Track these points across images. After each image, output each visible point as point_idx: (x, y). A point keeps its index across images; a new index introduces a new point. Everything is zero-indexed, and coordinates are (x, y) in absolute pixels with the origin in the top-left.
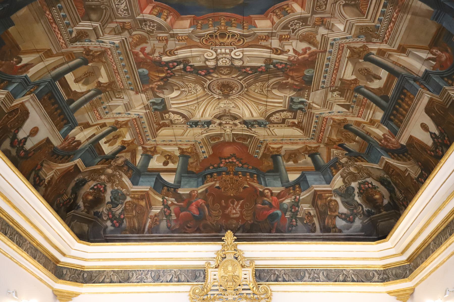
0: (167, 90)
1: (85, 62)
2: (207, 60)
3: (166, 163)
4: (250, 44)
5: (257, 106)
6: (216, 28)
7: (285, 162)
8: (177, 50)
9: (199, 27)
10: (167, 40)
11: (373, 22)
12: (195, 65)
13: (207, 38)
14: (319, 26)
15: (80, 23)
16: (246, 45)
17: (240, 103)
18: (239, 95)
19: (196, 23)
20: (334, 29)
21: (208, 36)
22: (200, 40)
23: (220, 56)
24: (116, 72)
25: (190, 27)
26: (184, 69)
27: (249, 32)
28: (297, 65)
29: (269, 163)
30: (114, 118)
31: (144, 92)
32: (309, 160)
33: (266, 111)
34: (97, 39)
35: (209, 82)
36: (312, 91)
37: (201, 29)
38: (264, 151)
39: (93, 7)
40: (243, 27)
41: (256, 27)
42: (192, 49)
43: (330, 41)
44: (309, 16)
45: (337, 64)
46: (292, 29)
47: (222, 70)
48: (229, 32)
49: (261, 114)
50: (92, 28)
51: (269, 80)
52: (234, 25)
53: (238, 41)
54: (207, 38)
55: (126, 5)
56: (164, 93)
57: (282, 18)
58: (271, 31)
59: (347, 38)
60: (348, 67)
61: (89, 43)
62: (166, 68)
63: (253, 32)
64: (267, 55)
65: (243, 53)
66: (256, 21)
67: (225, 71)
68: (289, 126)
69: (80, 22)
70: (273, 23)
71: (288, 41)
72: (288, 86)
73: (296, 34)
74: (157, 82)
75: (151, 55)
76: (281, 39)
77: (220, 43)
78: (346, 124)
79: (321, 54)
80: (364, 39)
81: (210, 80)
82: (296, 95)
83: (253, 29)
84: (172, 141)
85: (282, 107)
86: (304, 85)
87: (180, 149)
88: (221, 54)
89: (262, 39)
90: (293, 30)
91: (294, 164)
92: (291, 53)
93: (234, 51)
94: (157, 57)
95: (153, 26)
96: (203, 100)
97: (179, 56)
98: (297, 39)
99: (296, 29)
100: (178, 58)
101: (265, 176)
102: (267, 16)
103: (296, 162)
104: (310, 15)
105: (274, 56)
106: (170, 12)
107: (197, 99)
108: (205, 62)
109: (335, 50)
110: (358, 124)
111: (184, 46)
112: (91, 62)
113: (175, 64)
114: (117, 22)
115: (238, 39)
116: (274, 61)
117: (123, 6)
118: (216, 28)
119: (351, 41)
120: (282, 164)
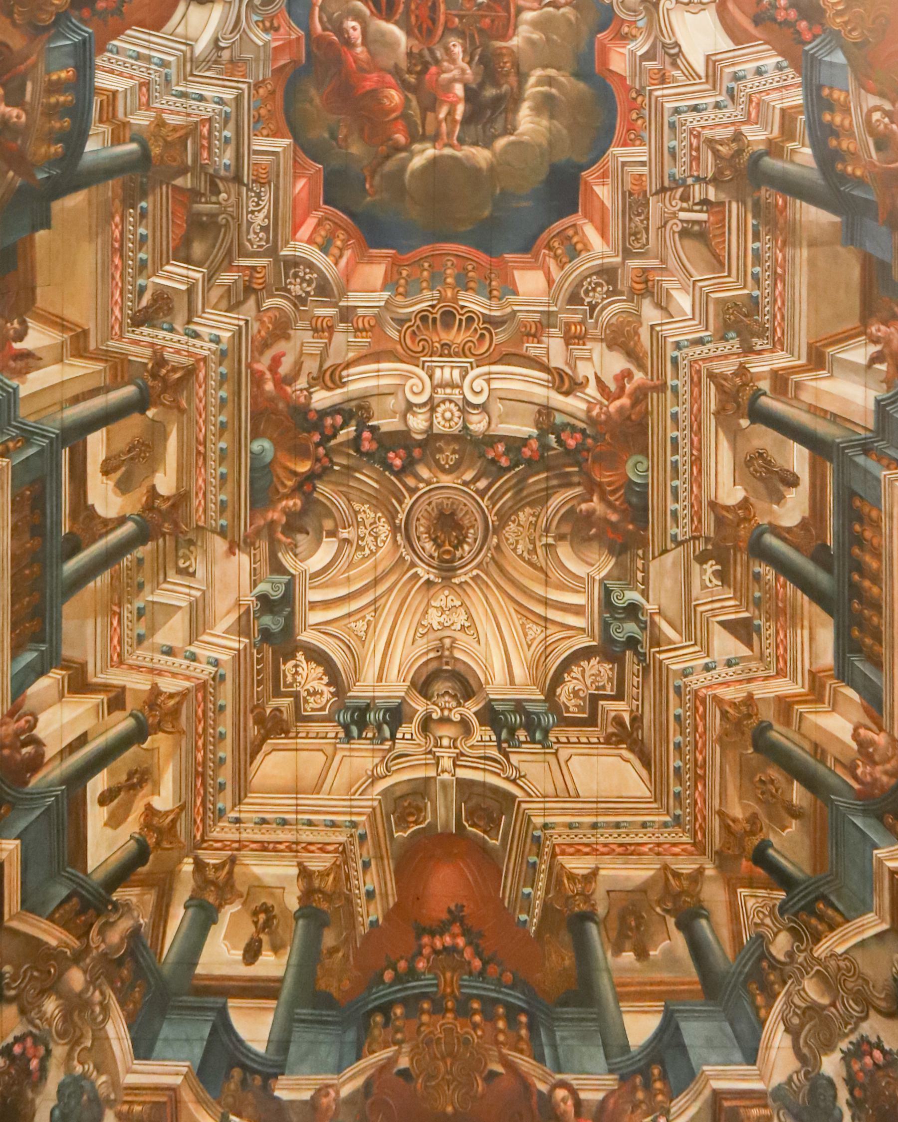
0: (308, 533)
1: (140, 404)
2: (410, 407)
3: (252, 953)
4: (505, 350)
5: (523, 625)
6: (436, 294)
7: (609, 954)
8: (348, 365)
9: (401, 290)
10: (331, 329)
11: (745, 287)
12: (384, 429)
13: (414, 328)
14: (642, 296)
15: (168, 268)
16: (496, 357)
17: (480, 610)
18: (478, 567)
19: (396, 277)
20: (672, 309)
21: (418, 322)
22: (400, 332)
23: (441, 394)
24: (199, 452)
25: (384, 288)
26: (356, 442)
27: (502, 308)
28: (607, 437)
29: (563, 959)
30: (151, 671)
31: (249, 544)
32: (679, 941)
33: (546, 654)
34: (189, 322)
35: (408, 502)
36: (654, 558)
37: (405, 295)
38: (547, 892)
39: (205, 219)
40: (490, 292)
41: (516, 293)
42: (384, 366)
43: (671, 353)
44: (617, 263)
45: (696, 439)
46: (590, 303)
47: (441, 450)
48: (463, 307)
49: (536, 666)
50: (184, 287)
51: (548, 497)
52: (472, 285)
53: (478, 340)
54: (414, 328)
55: (267, 217)
56: (298, 550)
57: (567, 267)
58: (546, 309)
59: (700, 342)
60: (720, 447)
61: (169, 335)
62: (317, 438)
63: (509, 310)
64: (542, 393)
65: (488, 381)
66: (516, 274)
67: (448, 457)
68: (608, 741)
69: (168, 263)
70: (550, 282)
71: (584, 344)
72: (593, 531)
73: (597, 321)
74: (287, 497)
75: (290, 385)
76: (570, 339)
77: (443, 346)
78: (753, 722)
79: (655, 395)
80: (734, 344)
81: (412, 491)
82: (616, 573)
83: (512, 298)
84: (284, 822)
85: (583, 630)
86: (631, 527)
87: (304, 873)
88: (443, 385)
89: (528, 335)
90: (593, 307)
91: (638, 965)
92: (592, 390)
93: (472, 374)
94: (301, 390)
95: (309, 283)
96: (390, 590)
97: (352, 387)
98: (602, 340)
99: (597, 304)
100: (346, 397)
101: (554, 1019)
102: (536, 257)
103: (642, 954)
104: (619, 259)
105: (558, 400)
106: (350, 237)
107: (376, 582)
108: (404, 417)
109: (682, 383)
110: (785, 705)
111: (364, 351)
112: (155, 405)
113: (339, 419)
114: (240, 268)
115: (479, 332)
116: (559, 419)
117: (262, 215)
118: (436, 294)
119: (712, 354)
120: (602, 964)
